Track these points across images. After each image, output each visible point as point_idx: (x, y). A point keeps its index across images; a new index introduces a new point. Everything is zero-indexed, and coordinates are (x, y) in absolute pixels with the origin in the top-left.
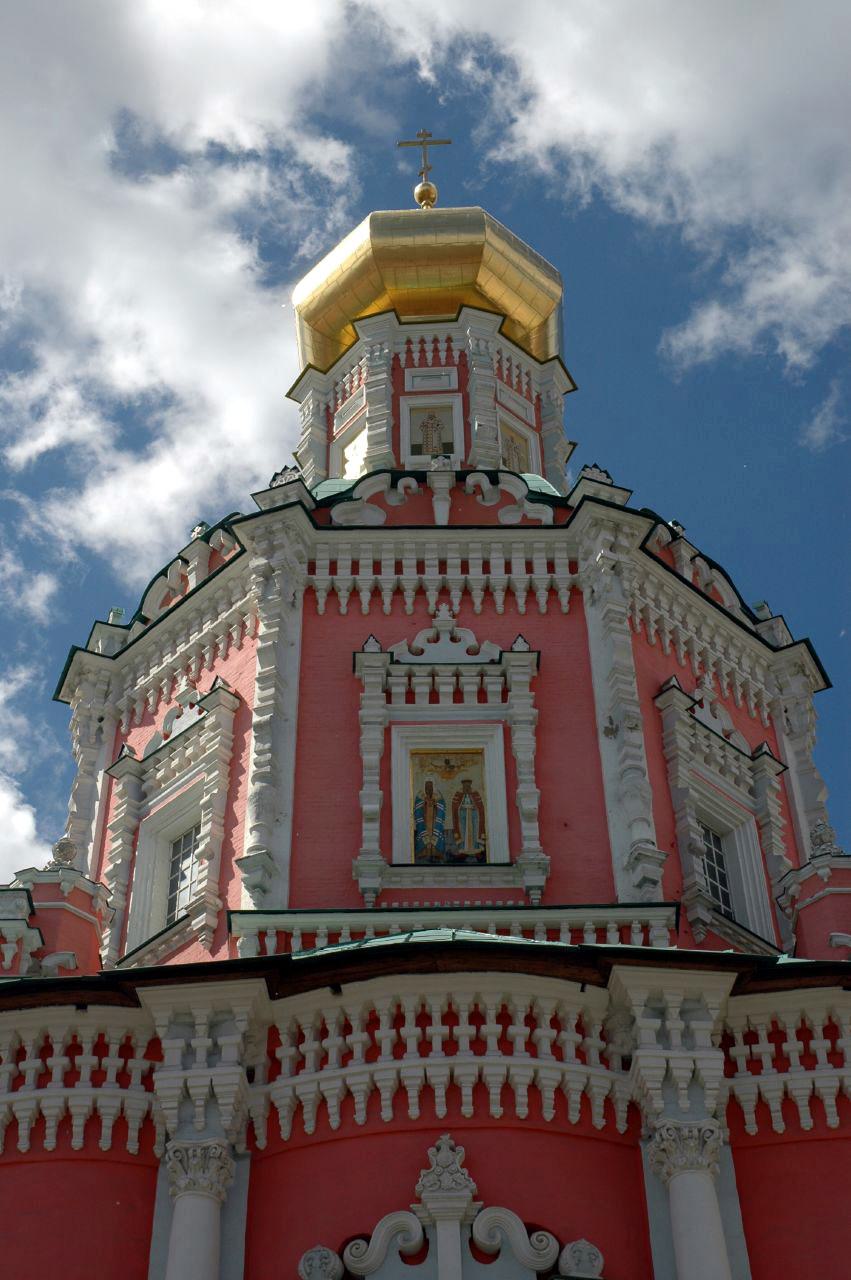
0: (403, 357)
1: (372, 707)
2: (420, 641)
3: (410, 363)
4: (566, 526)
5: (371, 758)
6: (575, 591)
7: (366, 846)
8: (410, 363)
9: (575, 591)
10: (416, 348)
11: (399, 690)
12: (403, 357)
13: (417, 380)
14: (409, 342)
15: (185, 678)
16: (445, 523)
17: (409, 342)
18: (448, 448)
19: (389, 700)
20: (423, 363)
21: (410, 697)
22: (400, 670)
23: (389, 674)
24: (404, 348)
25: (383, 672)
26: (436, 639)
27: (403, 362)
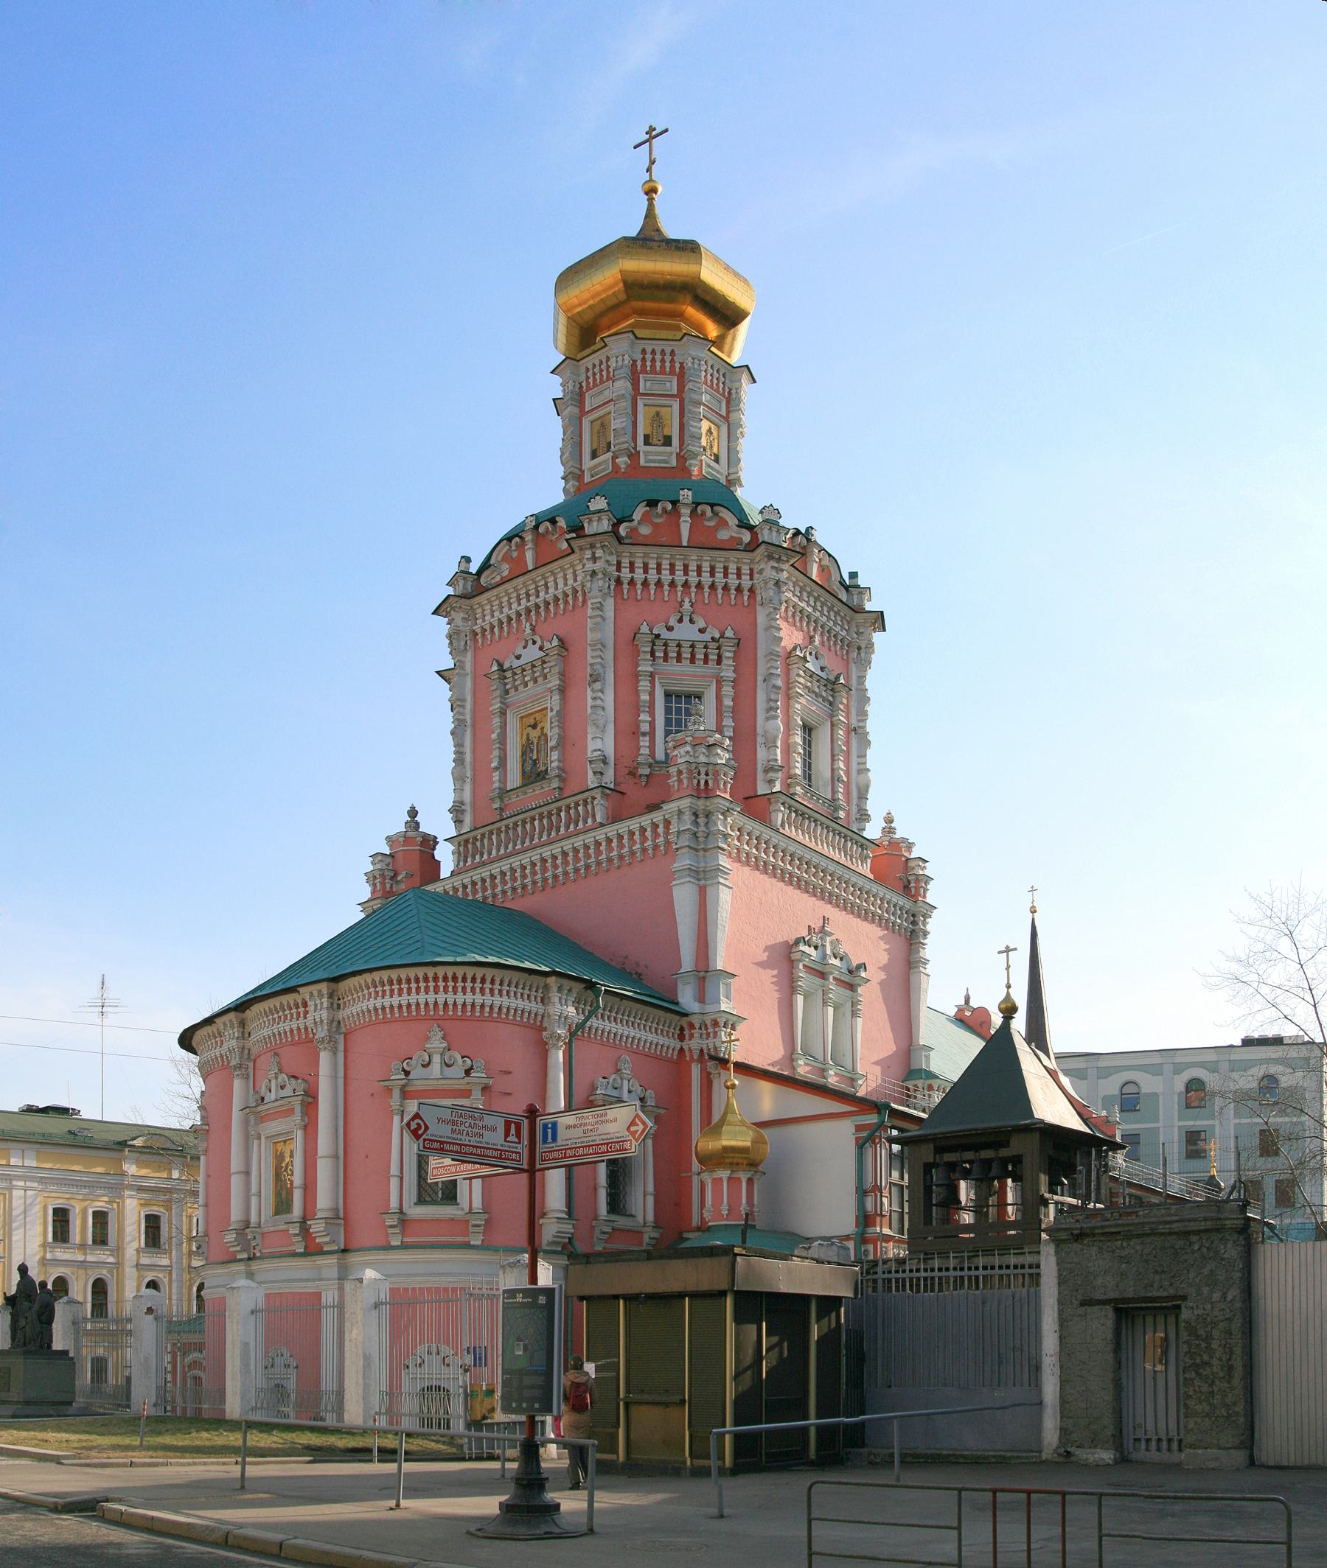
0: (639, 363)
1: (645, 667)
2: (672, 622)
3: (644, 371)
4: (752, 551)
5: (645, 697)
6: (751, 590)
7: (642, 751)
8: (644, 371)
9: (751, 590)
10: (649, 357)
11: (660, 654)
12: (639, 363)
13: (648, 384)
14: (644, 351)
15: (528, 625)
16: (686, 545)
17: (644, 351)
18: (667, 441)
19: (654, 660)
20: (653, 371)
21: (666, 658)
22: (657, 642)
23: (654, 645)
24: (639, 357)
25: (651, 644)
26: (680, 621)
27: (639, 368)
